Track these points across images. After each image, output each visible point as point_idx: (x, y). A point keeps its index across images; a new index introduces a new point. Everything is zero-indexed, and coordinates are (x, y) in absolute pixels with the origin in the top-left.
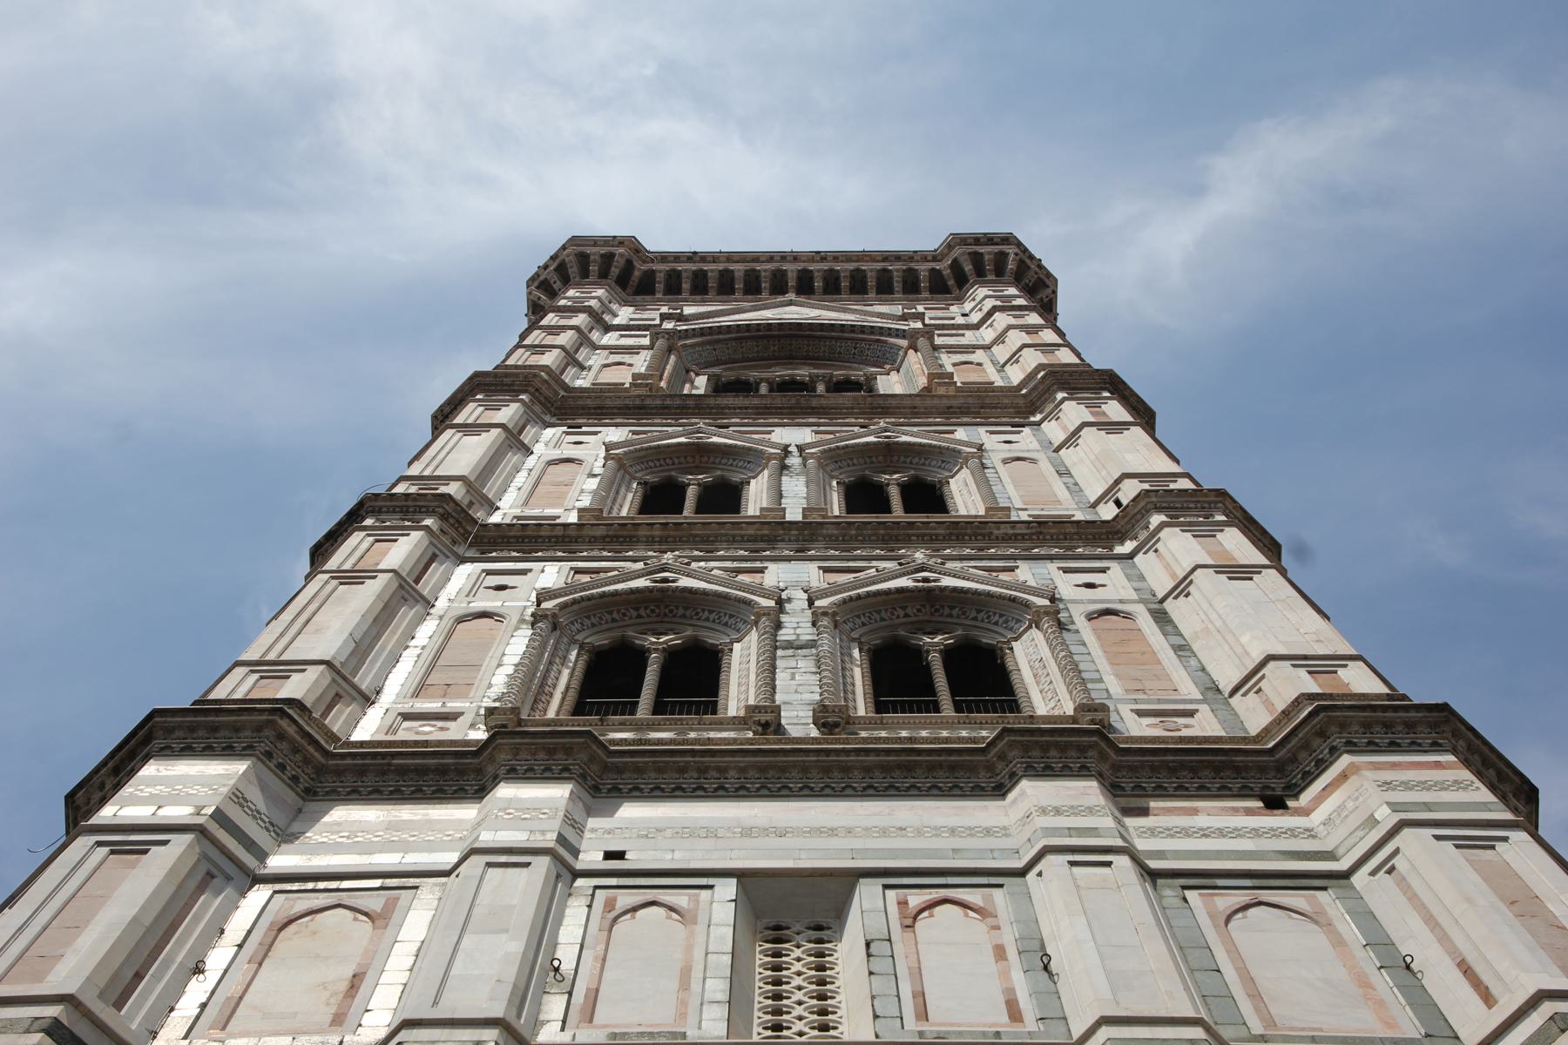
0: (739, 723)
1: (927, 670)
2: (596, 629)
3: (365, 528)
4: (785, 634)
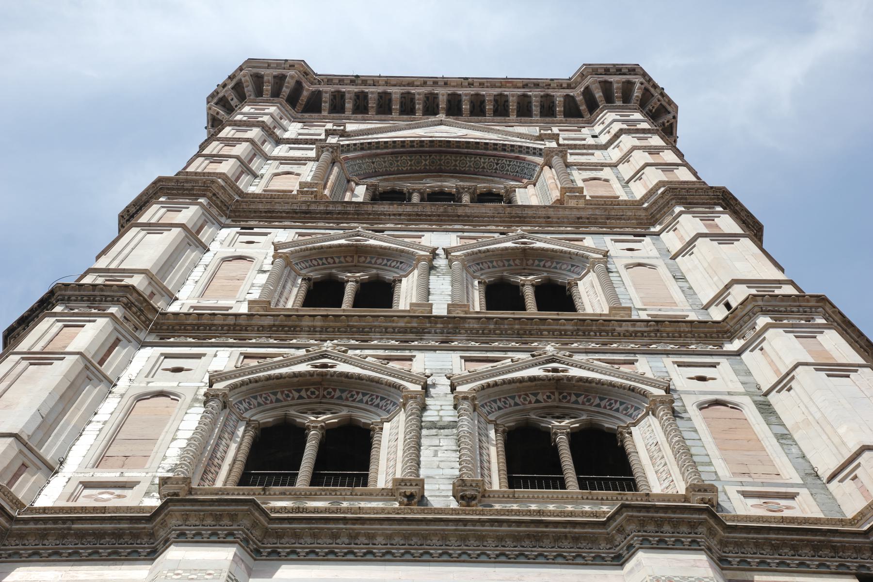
0: (387, 494)
1: (555, 451)
2: (261, 408)
3: (55, 315)
4: (430, 416)
